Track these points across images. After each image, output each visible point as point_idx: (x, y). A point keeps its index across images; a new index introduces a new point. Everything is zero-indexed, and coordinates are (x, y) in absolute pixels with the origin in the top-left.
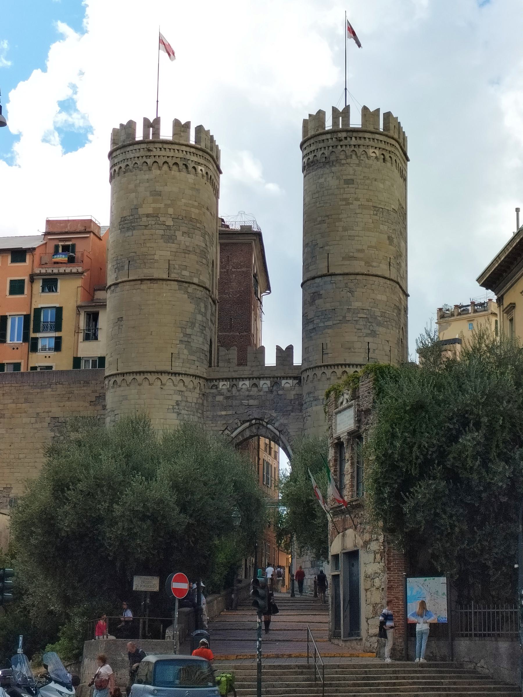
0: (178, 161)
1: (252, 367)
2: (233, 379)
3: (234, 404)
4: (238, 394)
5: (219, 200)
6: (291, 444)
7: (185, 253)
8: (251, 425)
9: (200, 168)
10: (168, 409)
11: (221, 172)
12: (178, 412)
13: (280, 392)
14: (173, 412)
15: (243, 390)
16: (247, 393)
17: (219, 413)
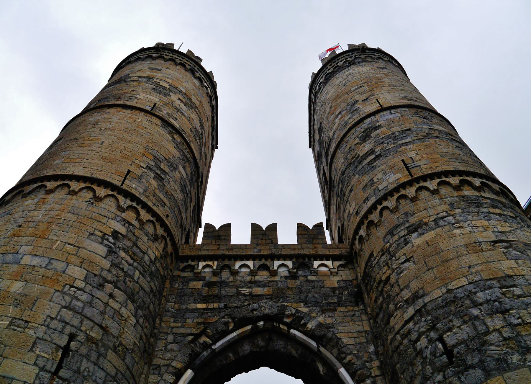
0: (187, 65)
1: (258, 244)
2: (223, 257)
3: (223, 292)
4: (231, 279)
5: (213, 161)
6: (346, 361)
7: (178, 111)
8: (256, 332)
9: (205, 84)
10: (92, 234)
11: (217, 148)
12: (110, 247)
13: (311, 278)
14: (101, 243)
15: (241, 274)
16: (249, 278)
17: (193, 306)
